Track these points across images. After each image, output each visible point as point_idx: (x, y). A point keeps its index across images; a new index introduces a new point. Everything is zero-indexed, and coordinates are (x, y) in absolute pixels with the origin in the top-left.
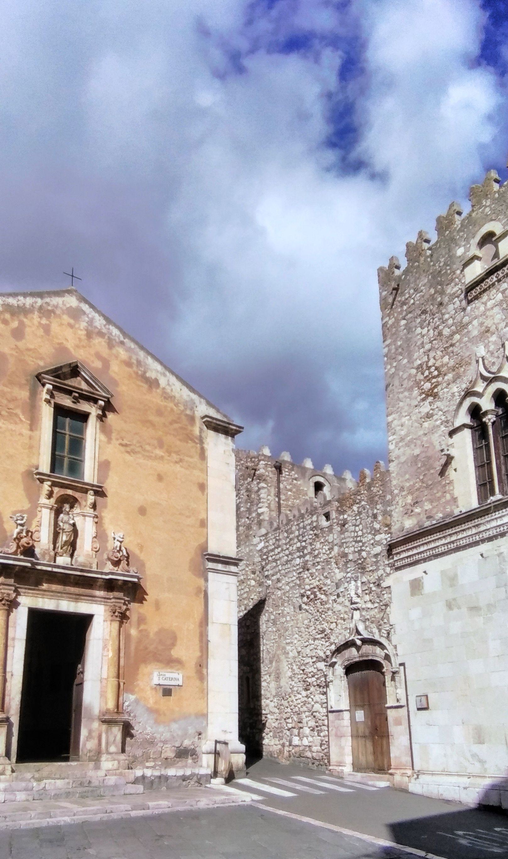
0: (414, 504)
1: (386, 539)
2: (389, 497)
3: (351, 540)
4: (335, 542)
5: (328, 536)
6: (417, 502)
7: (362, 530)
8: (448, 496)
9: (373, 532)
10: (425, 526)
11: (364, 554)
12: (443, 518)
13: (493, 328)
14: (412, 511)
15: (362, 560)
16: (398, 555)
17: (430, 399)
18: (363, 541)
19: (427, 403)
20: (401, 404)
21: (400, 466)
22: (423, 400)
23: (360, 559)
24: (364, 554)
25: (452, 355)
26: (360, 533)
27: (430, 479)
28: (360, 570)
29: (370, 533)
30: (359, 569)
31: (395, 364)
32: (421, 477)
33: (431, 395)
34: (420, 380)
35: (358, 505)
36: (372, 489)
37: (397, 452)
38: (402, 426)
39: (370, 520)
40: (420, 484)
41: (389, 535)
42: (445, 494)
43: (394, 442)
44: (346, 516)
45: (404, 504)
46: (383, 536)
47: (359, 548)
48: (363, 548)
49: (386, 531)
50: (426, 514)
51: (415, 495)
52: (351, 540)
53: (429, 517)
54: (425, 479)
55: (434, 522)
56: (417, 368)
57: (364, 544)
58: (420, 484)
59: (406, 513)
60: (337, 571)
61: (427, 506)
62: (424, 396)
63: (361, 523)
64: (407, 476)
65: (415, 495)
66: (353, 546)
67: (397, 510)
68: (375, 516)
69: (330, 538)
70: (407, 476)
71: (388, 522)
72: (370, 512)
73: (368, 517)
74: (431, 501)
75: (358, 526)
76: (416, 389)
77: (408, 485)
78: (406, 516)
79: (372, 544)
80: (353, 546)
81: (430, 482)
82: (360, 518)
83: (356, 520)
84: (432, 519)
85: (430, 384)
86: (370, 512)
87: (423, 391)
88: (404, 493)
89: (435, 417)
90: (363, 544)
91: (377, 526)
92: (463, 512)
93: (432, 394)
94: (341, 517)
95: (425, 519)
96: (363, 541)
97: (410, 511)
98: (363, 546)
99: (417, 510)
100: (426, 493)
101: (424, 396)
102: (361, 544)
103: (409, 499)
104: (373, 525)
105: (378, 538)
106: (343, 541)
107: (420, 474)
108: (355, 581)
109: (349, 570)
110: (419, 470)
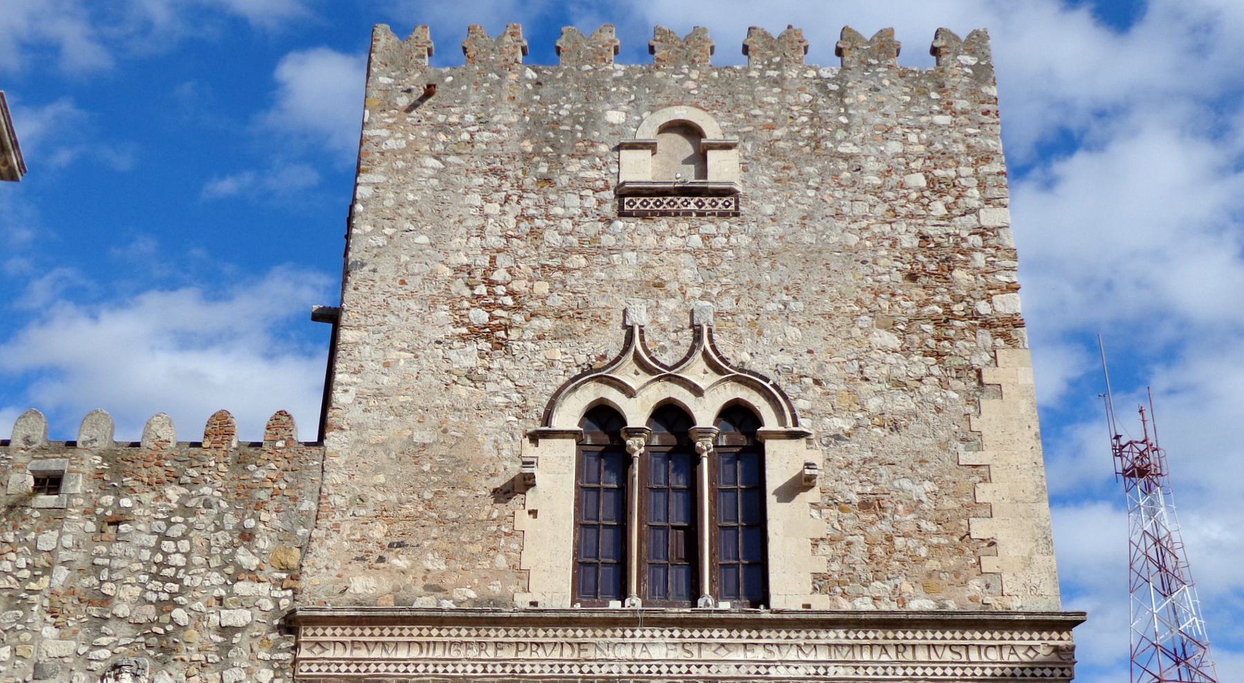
0: (391, 545)
1: (276, 601)
2: (308, 505)
3: (140, 566)
4: (64, 555)
5: (39, 531)
6: (400, 545)
7: (187, 555)
8: (501, 561)
9: (230, 570)
10: (415, 606)
11: (180, 615)
12: (475, 602)
13: (673, 287)
14: (381, 559)
15: (170, 628)
16: (317, 649)
17: (485, 346)
18: (186, 583)
19: (472, 348)
20: (392, 319)
21: (360, 448)
22: (462, 338)
23: (162, 626)
24: (180, 615)
25: (558, 286)
26: (178, 560)
27: (453, 508)
28: (152, 653)
29: (220, 569)
30: (148, 647)
31: (388, 231)
32: (428, 495)
33: (487, 338)
34: (462, 298)
35: (184, 490)
36: (252, 467)
37: (356, 414)
38: (386, 365)
39: (223, 538)
40: (421, 509)
41: (290, 593)
42: (492, 553)
43: (353, 390)
44: (126, 502)
45: (358, 536)
46: (264, 588)
47: (164, 597)
48: (179, 599)
49: (282, 580)
50: (425, 578)
51: (397, 527)
52: (140, 566)
53: (432, 589)
54: (439, 503)
55: (447, 604)
56: (458, 270)
57: (183, 590)
58: (421, 509)
59: (363, 559)
60: (49, 632)
61: (435, 564)
62: (464, 330)
63: (184, 537)
64: (381, 479)
65: (397, 527)
66: (143, 585)
67: (330, 543)
68: (247, 536)
69: (48, 540)
70: (381, 479)
71: (293, 563)
72: (230, 520)
73: (218, 529)
74: (449, 558)
75: (175, 540)
76: (447, 308)
77: (380, 497)
78: (361, 565)
79: (220, 600)
80: (143, 585)
81: (452, 515)
82: (185, 522)
83: (170, 524)
84: (440, 595)
85: (487, 315)
86: (230, 520)
87: (466, 320)
88: (363, 512)
89: (491, 387)
90: (182, 587)
91: (246, 558)
92: (540, 607)
93: (494, 336)
94: (108, 499)
95: (419, 589)
96: (187, 582)
97: (374, 558)
98: (179, 594)
99: (400, 562)
100: (435, 532)
101: (464, 330)
102: (175, 588)
103: (378, 531)
104: (234, 552)
105: (242, 588)
106: (97, 561)
107: (425, 486)
108: (135, 676)
109: (103, 641)
110: (421, 478)
